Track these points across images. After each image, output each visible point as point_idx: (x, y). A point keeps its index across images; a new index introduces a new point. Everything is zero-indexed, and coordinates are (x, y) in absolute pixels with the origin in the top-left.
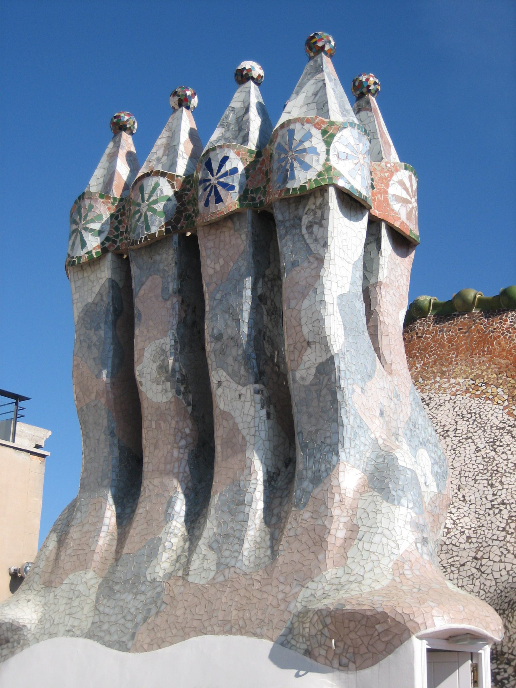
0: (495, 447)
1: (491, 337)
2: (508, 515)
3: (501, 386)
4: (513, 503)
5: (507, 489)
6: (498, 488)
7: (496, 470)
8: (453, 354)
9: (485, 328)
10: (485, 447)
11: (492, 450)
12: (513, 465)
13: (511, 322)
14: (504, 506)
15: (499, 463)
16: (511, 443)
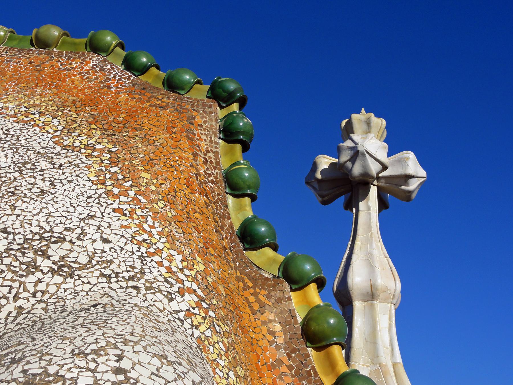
0: (23, 168)
1: (65, 75)
2: (6, 247)
3: (59, 118)
4: (19, 233)
5: (19, 216)
6: (5, 212)
7: (12, 192)
8: (13, 83)
9: (61, 65)
10: (9, 166)
11: (16, 171)
12: (40, 190)
13: (93, 65)
14: (5, 235)
15: (21, 185)
16: (47, 169)
